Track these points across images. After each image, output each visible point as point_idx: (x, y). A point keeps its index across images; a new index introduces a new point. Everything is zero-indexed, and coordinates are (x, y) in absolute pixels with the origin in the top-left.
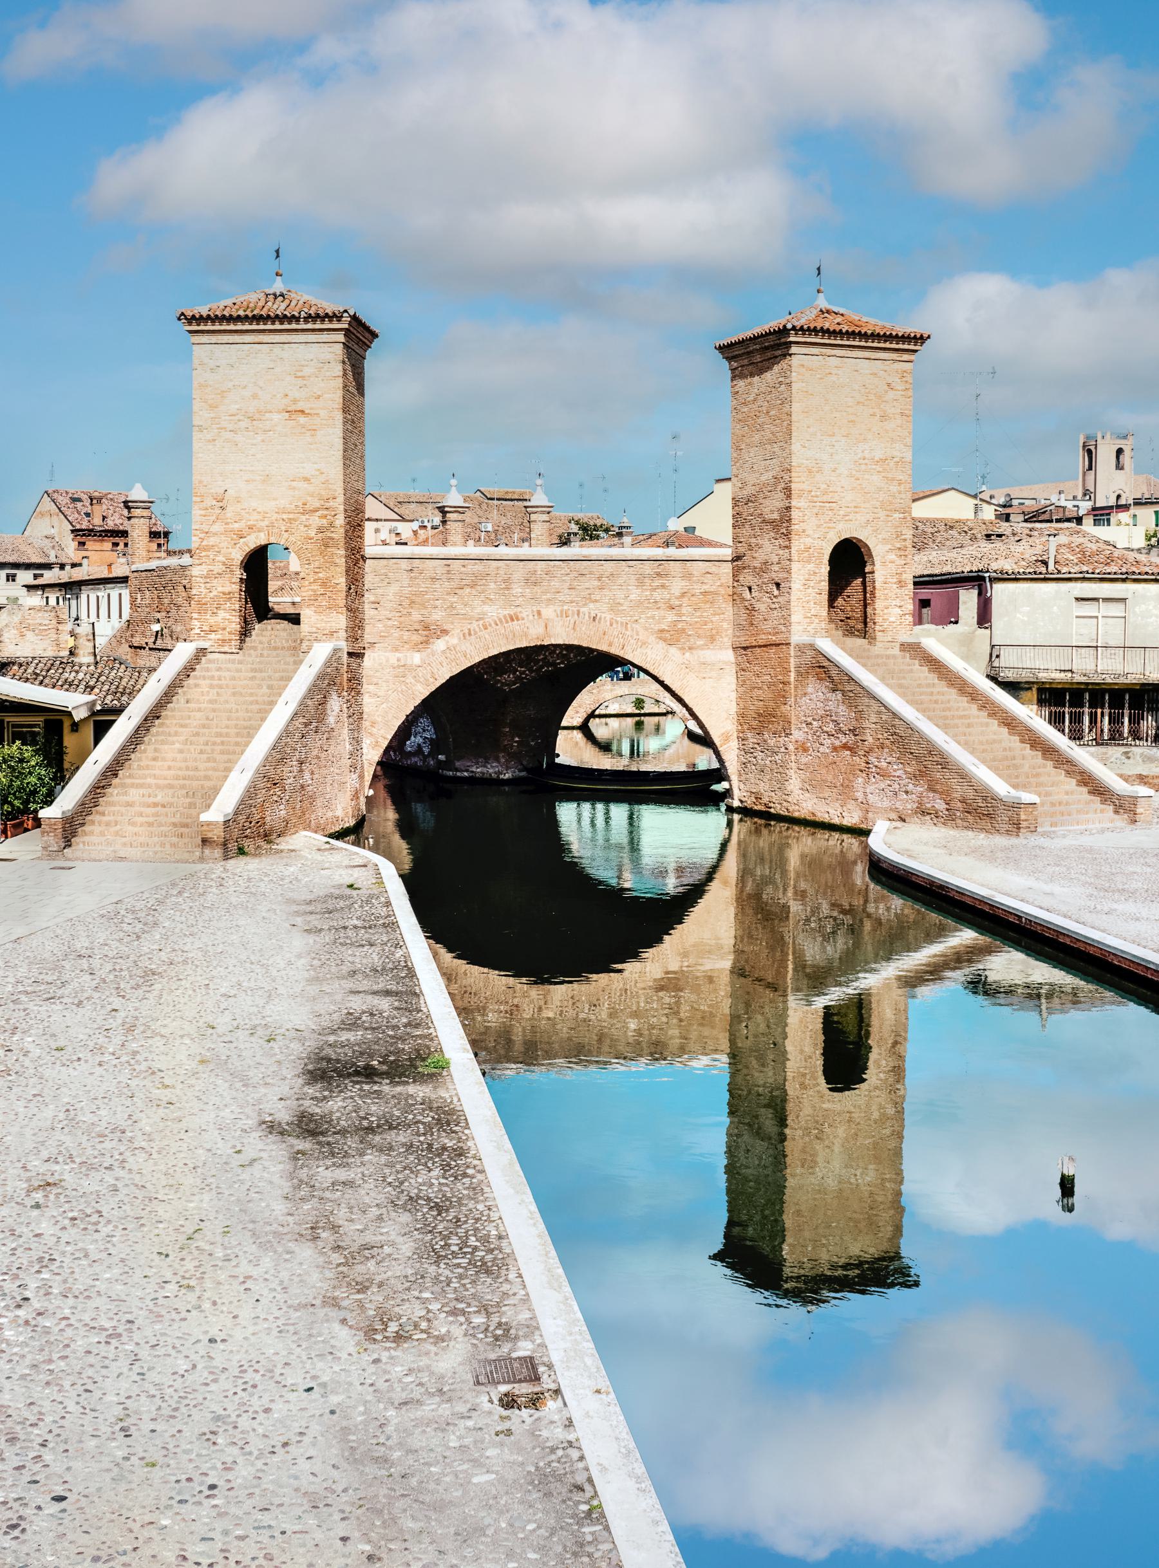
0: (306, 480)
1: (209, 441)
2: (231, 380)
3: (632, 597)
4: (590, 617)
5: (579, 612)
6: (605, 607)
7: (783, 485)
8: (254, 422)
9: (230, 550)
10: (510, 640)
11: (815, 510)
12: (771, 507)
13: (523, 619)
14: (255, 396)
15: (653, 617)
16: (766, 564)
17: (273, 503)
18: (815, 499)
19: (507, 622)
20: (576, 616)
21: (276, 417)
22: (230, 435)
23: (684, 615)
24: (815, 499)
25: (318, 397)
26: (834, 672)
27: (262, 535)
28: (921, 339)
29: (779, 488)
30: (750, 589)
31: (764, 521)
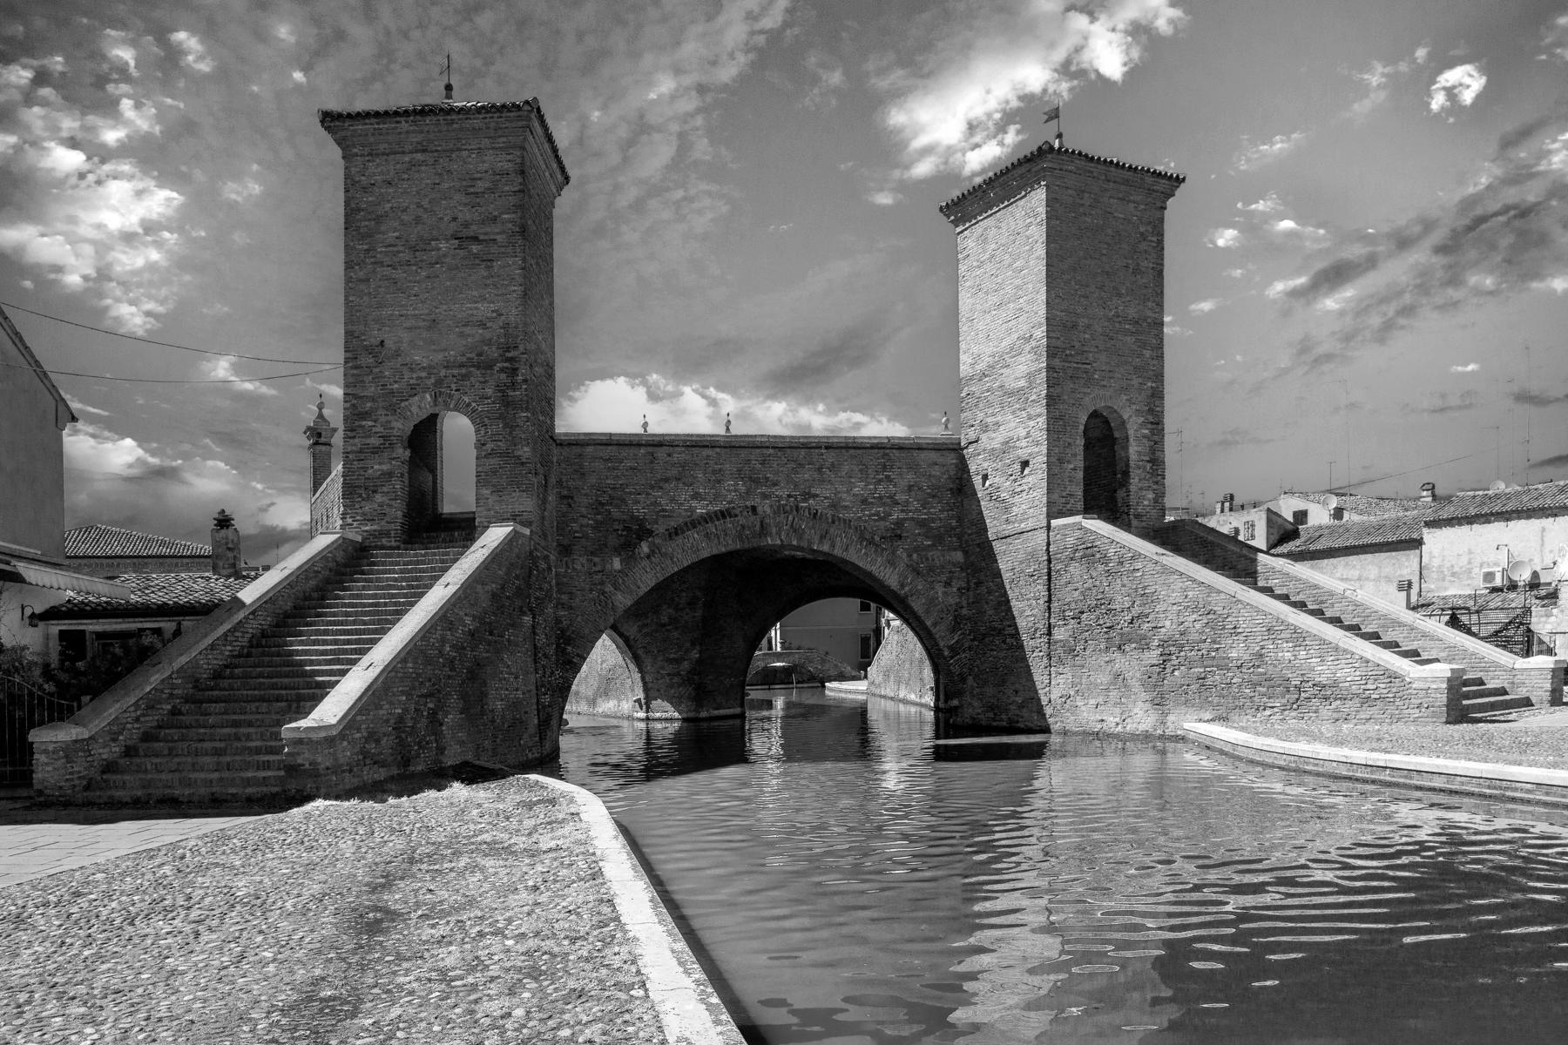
1: (361, 281)
2: (388, 201)
4: (810, 514)
5: (797, 507)
7: (1034, 343)
8: (417, 253)
9: (390, 418)
10: (722, 540)
11: (1070, 372)
13: (736, 516)
14: (418, 220)
15: (877, 514)
18: (1070, 359)
19: (718, 520)
20: (795, 512)
22: (387, 271)
23: (910, 511)
24: (1070, 359)
29: (1028, 348)
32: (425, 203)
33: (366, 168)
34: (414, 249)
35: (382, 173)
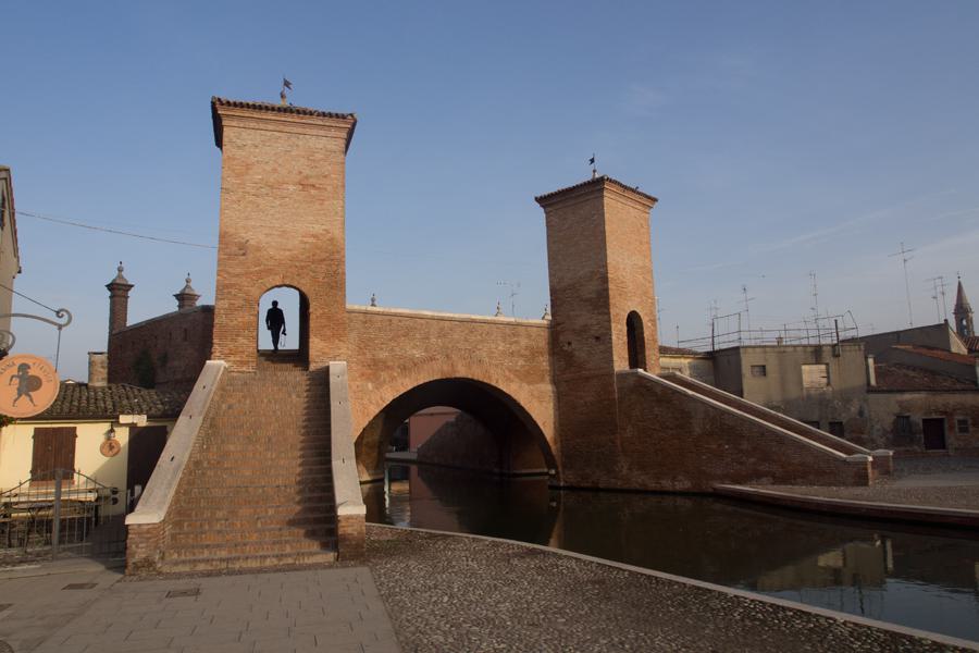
0: (314, 236)
3: (500, 348)
6: (485, 354)
7: (598, 276)
12: (589, 290)
14: (275, 170)
16: (585, 329)
17: (288, 253)
21: (291, 188)
22: (252, 198)
25: (325, 177)
26: (658, 390)
27: (278, 277)
28: (655, 200)
30: (569, 344)
31: (582, 300)
32: (280, 161)
33: (240, 134)
34: (272, 187)
35: (251, 140)
